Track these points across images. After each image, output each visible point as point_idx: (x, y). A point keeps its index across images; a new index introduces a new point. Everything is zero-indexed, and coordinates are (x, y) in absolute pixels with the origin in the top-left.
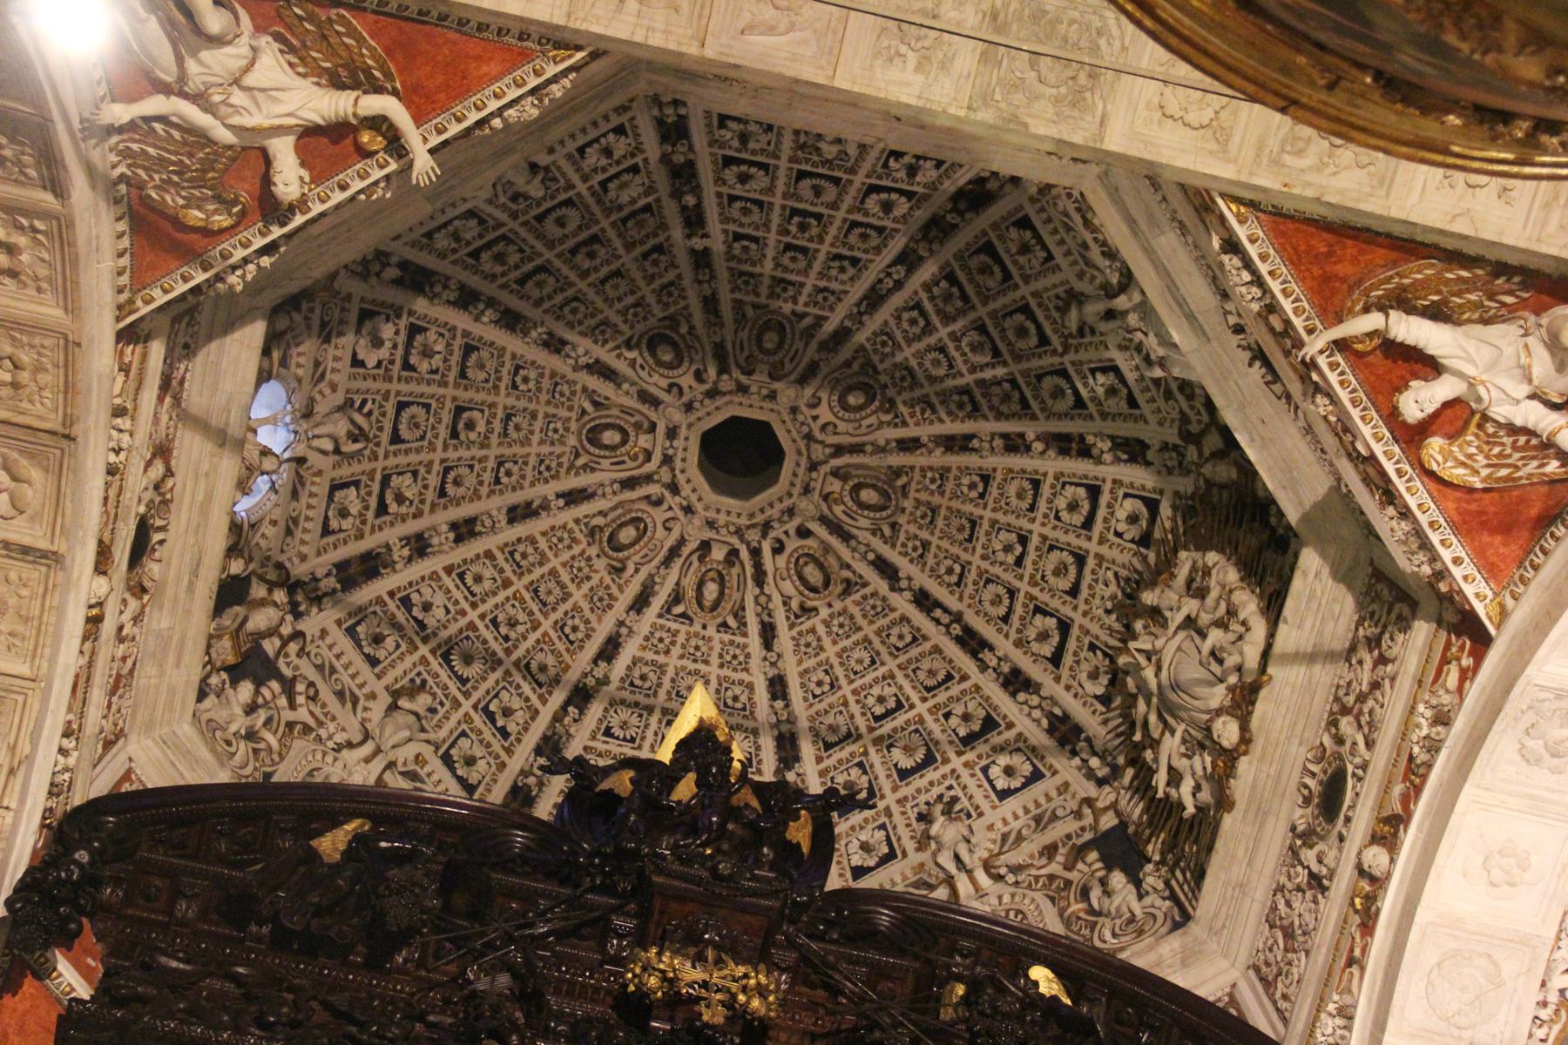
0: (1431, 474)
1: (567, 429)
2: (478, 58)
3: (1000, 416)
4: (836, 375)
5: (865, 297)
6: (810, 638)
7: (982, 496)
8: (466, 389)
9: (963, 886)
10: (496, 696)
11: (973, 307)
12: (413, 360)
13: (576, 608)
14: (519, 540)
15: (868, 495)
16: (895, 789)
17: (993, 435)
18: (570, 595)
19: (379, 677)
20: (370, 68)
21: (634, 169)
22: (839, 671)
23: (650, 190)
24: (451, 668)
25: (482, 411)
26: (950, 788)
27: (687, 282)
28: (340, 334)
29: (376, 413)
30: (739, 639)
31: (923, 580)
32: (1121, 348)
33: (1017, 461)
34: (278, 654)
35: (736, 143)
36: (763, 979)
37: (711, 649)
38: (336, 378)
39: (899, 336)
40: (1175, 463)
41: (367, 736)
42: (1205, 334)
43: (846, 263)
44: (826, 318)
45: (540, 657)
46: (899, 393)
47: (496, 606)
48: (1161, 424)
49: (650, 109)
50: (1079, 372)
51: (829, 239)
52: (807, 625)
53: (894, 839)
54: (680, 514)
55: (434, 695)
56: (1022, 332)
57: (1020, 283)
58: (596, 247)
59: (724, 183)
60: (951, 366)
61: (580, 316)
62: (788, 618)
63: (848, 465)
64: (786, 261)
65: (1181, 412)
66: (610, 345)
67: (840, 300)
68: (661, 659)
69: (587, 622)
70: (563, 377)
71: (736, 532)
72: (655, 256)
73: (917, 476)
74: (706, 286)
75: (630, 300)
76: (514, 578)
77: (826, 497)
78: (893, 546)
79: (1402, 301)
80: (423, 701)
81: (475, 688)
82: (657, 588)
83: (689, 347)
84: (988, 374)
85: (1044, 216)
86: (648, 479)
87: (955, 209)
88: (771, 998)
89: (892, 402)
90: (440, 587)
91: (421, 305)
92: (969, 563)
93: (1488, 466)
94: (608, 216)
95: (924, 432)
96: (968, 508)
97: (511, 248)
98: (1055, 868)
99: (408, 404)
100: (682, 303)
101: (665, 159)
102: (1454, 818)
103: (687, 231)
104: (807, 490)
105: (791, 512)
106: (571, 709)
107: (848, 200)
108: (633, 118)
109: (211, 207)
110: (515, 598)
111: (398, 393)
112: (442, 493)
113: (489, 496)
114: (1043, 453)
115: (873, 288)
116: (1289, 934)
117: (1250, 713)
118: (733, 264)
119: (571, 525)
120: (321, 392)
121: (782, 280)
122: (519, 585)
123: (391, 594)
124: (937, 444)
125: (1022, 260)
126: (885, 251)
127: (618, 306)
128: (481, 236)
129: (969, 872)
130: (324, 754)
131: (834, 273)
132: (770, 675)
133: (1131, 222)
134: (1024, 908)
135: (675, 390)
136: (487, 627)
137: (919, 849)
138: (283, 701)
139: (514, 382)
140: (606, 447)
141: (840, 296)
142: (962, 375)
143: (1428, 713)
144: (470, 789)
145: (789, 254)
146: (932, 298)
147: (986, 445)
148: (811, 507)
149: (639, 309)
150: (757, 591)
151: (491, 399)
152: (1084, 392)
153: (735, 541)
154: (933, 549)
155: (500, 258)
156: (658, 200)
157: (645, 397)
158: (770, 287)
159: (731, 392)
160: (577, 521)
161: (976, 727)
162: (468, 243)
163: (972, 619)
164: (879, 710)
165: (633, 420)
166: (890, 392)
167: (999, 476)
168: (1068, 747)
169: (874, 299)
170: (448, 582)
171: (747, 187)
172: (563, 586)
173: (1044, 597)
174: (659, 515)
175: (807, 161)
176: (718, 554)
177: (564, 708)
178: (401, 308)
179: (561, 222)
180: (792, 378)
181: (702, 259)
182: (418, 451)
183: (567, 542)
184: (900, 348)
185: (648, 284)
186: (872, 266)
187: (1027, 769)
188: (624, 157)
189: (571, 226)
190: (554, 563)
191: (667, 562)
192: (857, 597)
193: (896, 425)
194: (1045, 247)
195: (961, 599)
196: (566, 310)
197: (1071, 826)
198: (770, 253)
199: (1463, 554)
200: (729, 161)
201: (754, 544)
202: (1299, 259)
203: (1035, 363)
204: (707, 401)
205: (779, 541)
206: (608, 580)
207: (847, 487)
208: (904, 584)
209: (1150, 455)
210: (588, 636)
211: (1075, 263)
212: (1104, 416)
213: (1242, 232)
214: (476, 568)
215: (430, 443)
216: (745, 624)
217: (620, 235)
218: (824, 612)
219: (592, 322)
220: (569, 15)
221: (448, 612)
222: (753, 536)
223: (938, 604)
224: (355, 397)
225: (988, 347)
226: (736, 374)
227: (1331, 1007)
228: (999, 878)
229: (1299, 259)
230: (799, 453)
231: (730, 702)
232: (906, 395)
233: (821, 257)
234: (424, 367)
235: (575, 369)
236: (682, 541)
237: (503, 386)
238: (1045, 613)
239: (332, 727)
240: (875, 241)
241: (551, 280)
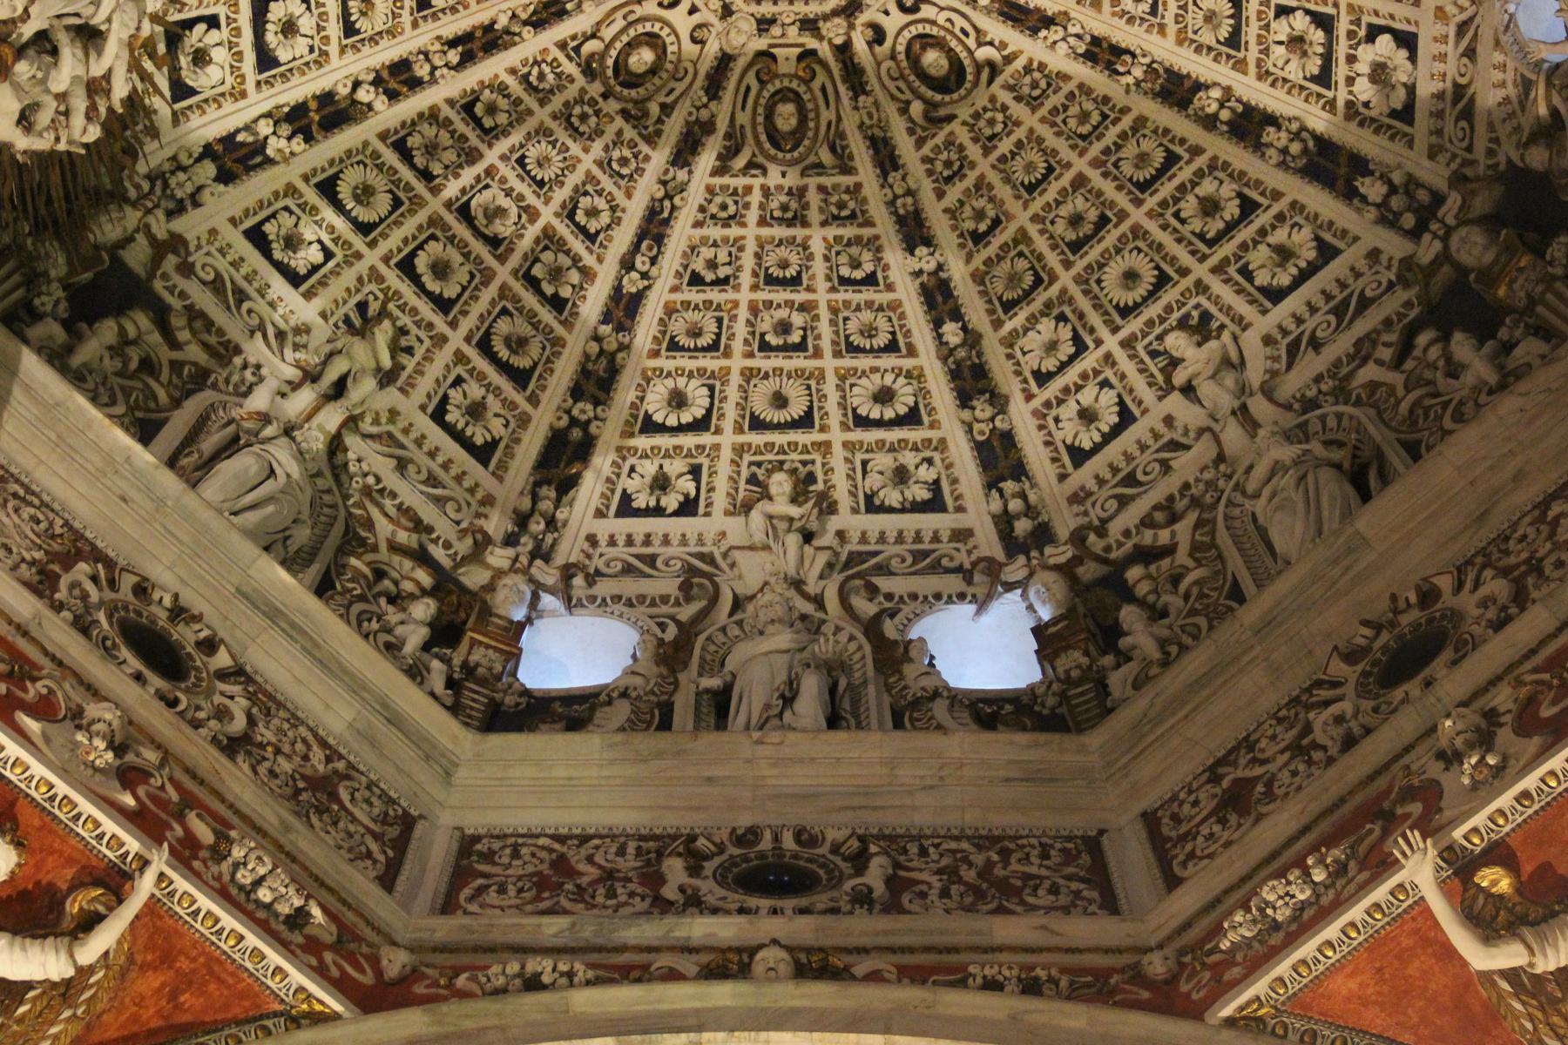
2: (1365, 1003)
3: (432, 116)
11: (515, 273)
12: (1319, 36)
17: (433, 81)
20: (1517, 995)
23: (1009, 342)
27: (927, 188)
28: (1440, 96)
32: (303, 330)
33: (388, 52)
38: (1439, 29)
39: (607, 183)
40: (173, 182)
42: (247, 597)
43: (709, 277)
44: (716, 172)
46: (583, 91)
49: (1042, 499)
51: (743, 313)
56: (441, 270)
58: (1071, 236)
59: (909, 375)
66: (1019, 64)
67: (702, 209)
72: (983, 227)
74: (899, 191)
75: (1005, 146)
79: (65, 991)
83: (902, 77)
84: (468, 175)
85: (467, 483)
89: (589, 72)
91: (1318, 121)
95: (533, 44)
100: (926, 150)
101: (1000, 403)
103: (943, 275)
108: (1063, 477)
114: (357, 85)
115: (659, 240)
118: (866, 232)
121: (790, 223)
124: (507, 32)
126: (660, 313)
127: (1020, 133)
131: (722, 257)
133: (395, 720)
141: (705, 216)
145: (791, 272)
146: (576, 259)
147: (438, 61)
149: (988, 132)
152: (329, 214)
158: (806, 206)
159: (826, 17)
166: (596, 89)
169: (654, 228)
178: (1348, 118)
181: (915, 232)
184: (599, 164)
185: (982, 177)
186: (672, 281)
194: (450, 429)
198: (819, 267)
209: (209, 169)
211: (406, 431)
217: (1040, 258)
219: (1055, 100)
225: (481, 221)
226: (824, 50)
229: (211, 972)
232: (571, 92)
233: (746, 279)
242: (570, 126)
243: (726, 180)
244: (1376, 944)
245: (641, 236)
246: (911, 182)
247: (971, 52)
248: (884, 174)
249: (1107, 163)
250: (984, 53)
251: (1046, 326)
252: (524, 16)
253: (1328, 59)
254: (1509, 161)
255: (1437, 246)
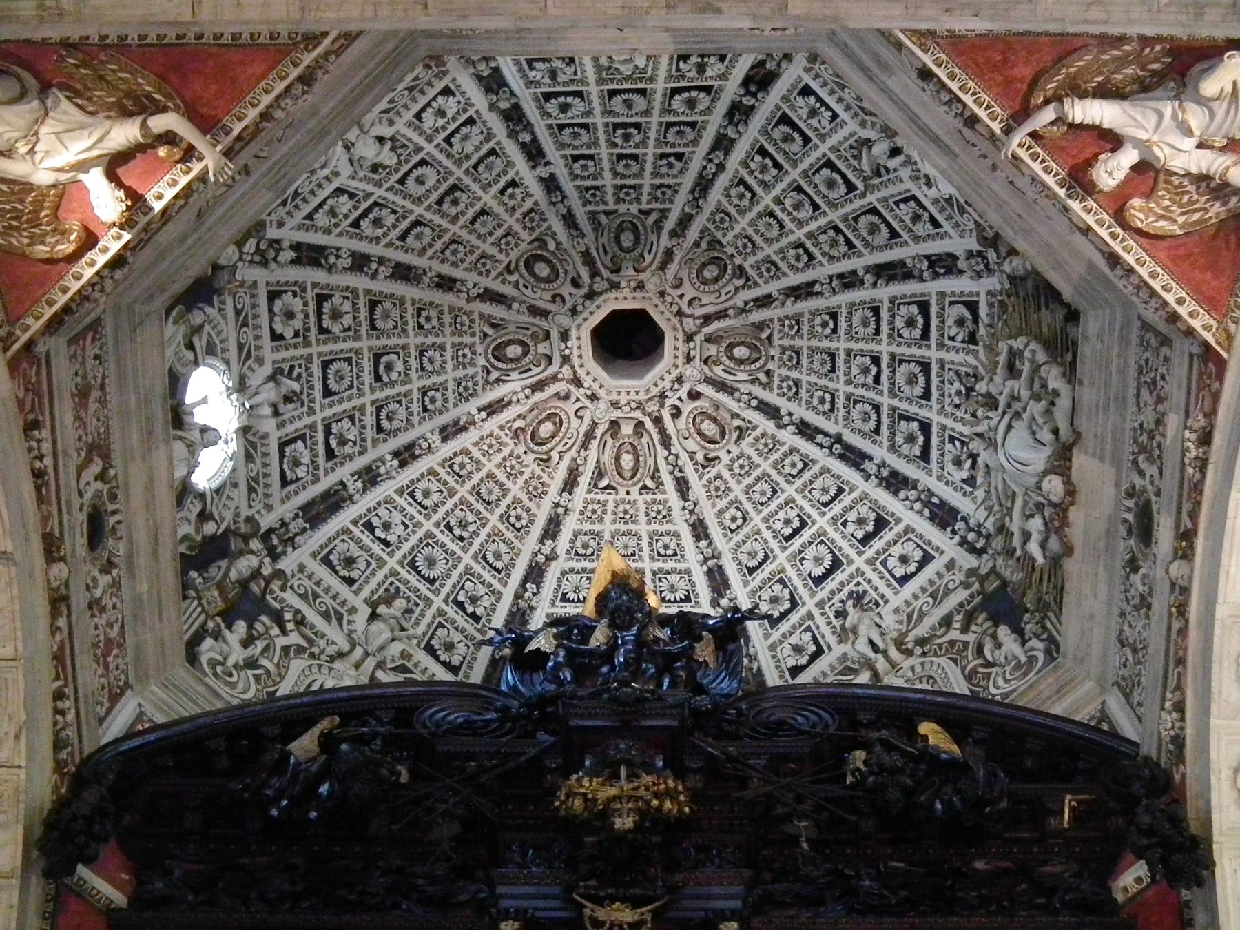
0: (1139, 232)
1: (474, 353)
2: (241, 62)
4: (690, 256)
5: (697, 184)
6: (718, 483)
7: (834, 331)
8: (378, 338)
9: (881, 664)
10: (462, 588)
13: (517, 501)
14: (455, 454)
15: (740, 352)
16: (813, 594)
17: (831, 277)
18: (509, 490)
19: (356, 593)
20: (150, 92)
21: (470, 122)
22: (748, 506)
24: (419, 573)
25: (398, 354)
26: (858, 584)
29: (304, 375)
30: (659, 497)
31: (801, 412)
34: (264, 593)
35: (547, 80)
36: (671, 783)
37: (637, 510)
39: (733, 211)
40: (982, 267)
41: (353, 645)
43: (672, 159)
44: (669, 210)
45: (492, 547)
47: (447, 514)
48: (962, 236)
49: (466, 68)
50: (887, 207)
51: (651, 142)
52: (714, 472)
53: (819, 638)
54: (587, 403)
55: (408, 599)
56: (831, 185)
57: (818, 142)
59: (549, 115)
60: (782, 227)
61: (460, 255)
62: (697, 470)
63: (718, 330)
64: (620, 169)
65: (976, 222)
67: (676, 192)
68: (597, 527)
69: (528, 510)
70: (460, 309)
71: (638, 408)
72: (510, 190)
73: (776, 325)
74: (560, 205)
75: (499, 232)
76: (457, 487)
77: (706, 362)
78: (771, 390)
80: (400, 603)
81: (442, 585)
82: (580, 469)
83: (561, 261)
86: (554, 378)
87: (748, 93)
88: (682, 798)
90: (395, 508)
92: (837, 390)
93: (1183, 213)
94: (459, 166)
95: (773, 288)
96: (825, 344)
97: (385, 212)
98: (954, 634)
99: (331, 362)
100: (545, 225)
102: (1229, 522)
103: (531, 163)
104: (689, 359)
105: (679, 380)
106: (528, 585)
107: (657, 106)
108: (454, 80)
109: (53, 240)
110: (462, 503)
111: (319, 354)
112: (380, 429)
113: (420, 423)
115: (701, 176)
116: (1135, 651)
117: (1070, 468)
118: (578, 182)
119: (497, 432)
120: (250, 368)
121: (623, 187)
122: (463, 491)
123: (355, 523)
124: (788, 296)
125: (814, 122)
127: (490, 240)
128: (356, 208)
129: (885, 653)
130: (320, 666)
131: (664, 170)
132: (691, 522)
133: (864, 70)
134: (932, 673)
135: (558, 299)
136: (442, 532)
137: (840, 642)
138: (275, 631)
139: (419, 323)
140: (512, 360)
141: (673, 188)
142: (793, 232)
143: (1194, 437)
144: (454, 670)
146: (751, 172)
148: (696, 372)
149: (510, 238)
150: (666, 453)
151: (401, 341)
153: (638, 414)
154: (804, 385)
155: (377, 222)
156: (498, 143)
157: (535, 311)
158: (614, 194)
159: (606, 291)
160: (501, 428)
161: (870, 528)
162: (346, 216)
163: (851, 438)
164: (788, 531)
165: (529, 333)
167: (844, 311)
168: (949, 530)
170: (401, 502)
171: (569, 114)
172: (501, 485)
173: (904, 406)
174: (570, 407)
175: (612, 80)
176: (627, 429)
177: (523, 586)
179: (420, 181)
180: (654, 267)
182: (350, 399)
183: (495, 448)
187: (918, 555)
188: (458, 113)
189: (430, 183)
190: (489, 466)
191: (585, 446)
192: (750, 440)
193: (750, 287)
194: (828, 108)
195: (837, 423)
196: (448, 253)
197: (962, 595)
198: (606, 165)
199: (1184, 295)
200: (548, 96)
201: (655, 414)
202: (981, 71)
203: (849, 208)
204: (588, 303)
205: (676, 407)
206: (538, 471)
207: (722, 349)
208: (786, 420)
209: (961, 264)
210: (532, 522)
212: (917, 239)
213: (928, 60)
214: (423, 485)
215: (359, 389)
216: (662, 484)
217: (475, 180)
218: (725, 458)
219: (473, 258)
220: (302, 9)
221: (406, 527)
222: (652, 407)
223: (818, 431)
224: (283, 366)
226: (605, 273)
227: (1168, 705)
228: (909, 653)
229: (981, 71)
230: (675, 329)
231: (662, 551)
233: (650, 159)
234: (336, 329)
235: (468, 300)
236: (594, 425)
237: (410, 328)
238: (909, 419)
239: (322, 643)
240: (690, 134)
241: (427, 231)
242: (753, 243)
243: (661, 206)
244: (239, 97)
245: (711, 182)
246: (553, 210)
247: (521, 276)
248: (569, 211)
249: (439, 233)
250: (514, 278)
251: (469, 149)
252: (776, 303)
253: (319, 313)
254: (211, 305)
255: (245, 250)
